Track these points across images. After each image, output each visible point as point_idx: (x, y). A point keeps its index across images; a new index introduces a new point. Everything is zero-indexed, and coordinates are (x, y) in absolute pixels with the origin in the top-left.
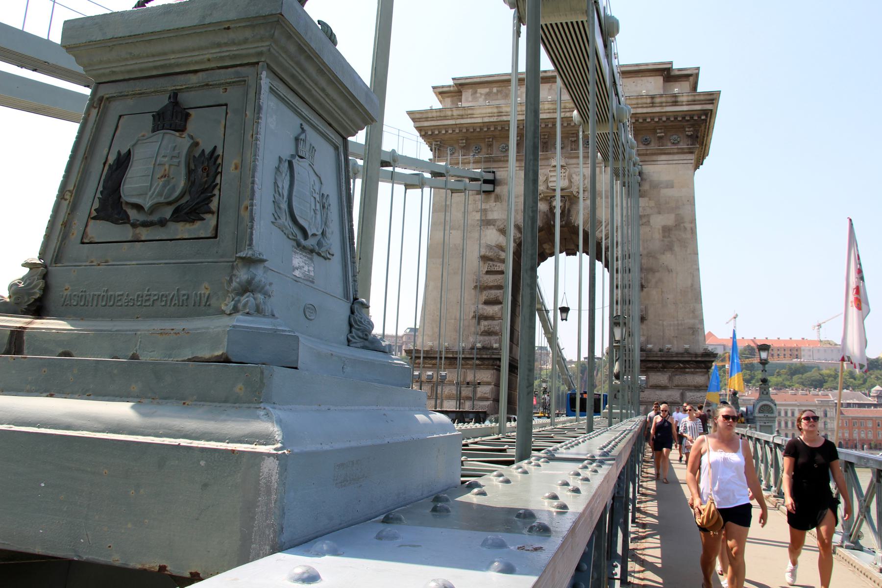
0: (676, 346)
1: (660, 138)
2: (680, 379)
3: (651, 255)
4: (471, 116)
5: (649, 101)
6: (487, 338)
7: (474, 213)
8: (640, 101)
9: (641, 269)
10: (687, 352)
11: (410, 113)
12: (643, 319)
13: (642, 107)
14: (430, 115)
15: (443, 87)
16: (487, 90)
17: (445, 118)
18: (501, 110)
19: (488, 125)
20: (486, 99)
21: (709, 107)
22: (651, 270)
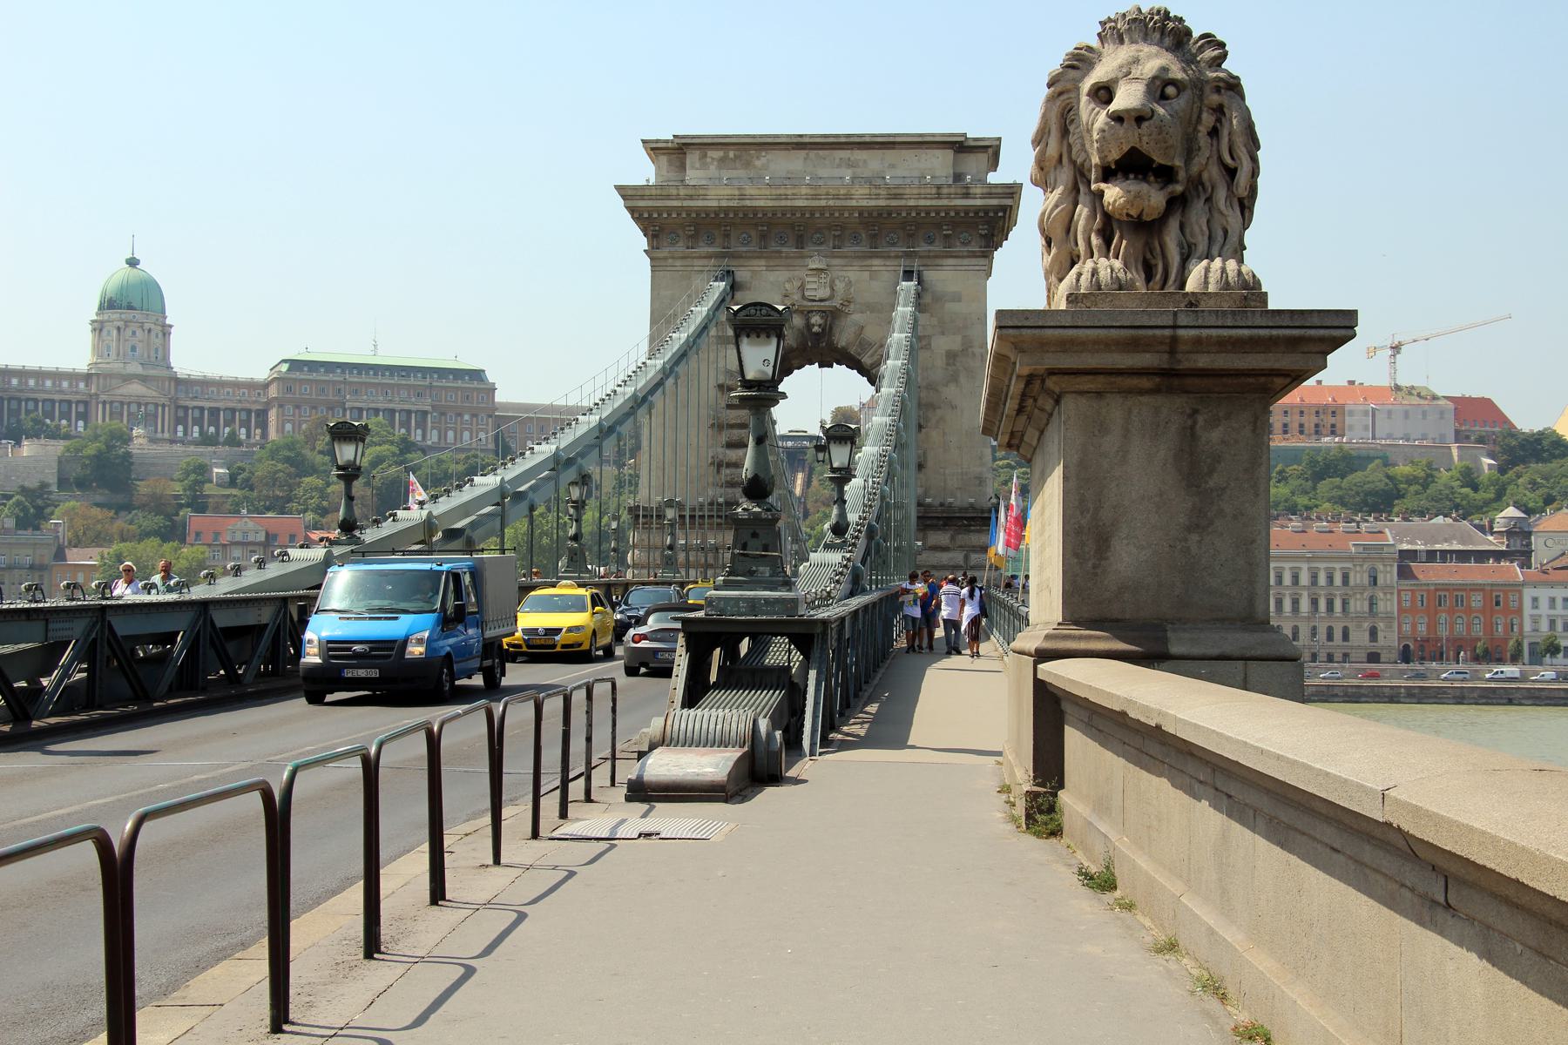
0: (960, 500)
2: (963, 539)
3: (931, 387)
4: (704, 197)
6: (730, 490)
9: (919, 405)
10: (972, 506)
11: (619, 188)
12: (920, 467)
15: (657, 141)
16: (721, 154)
17: (668, 197)
19: (727, 210)
20: (719, 168)
21: (1008, 202)
22: (932, 406)
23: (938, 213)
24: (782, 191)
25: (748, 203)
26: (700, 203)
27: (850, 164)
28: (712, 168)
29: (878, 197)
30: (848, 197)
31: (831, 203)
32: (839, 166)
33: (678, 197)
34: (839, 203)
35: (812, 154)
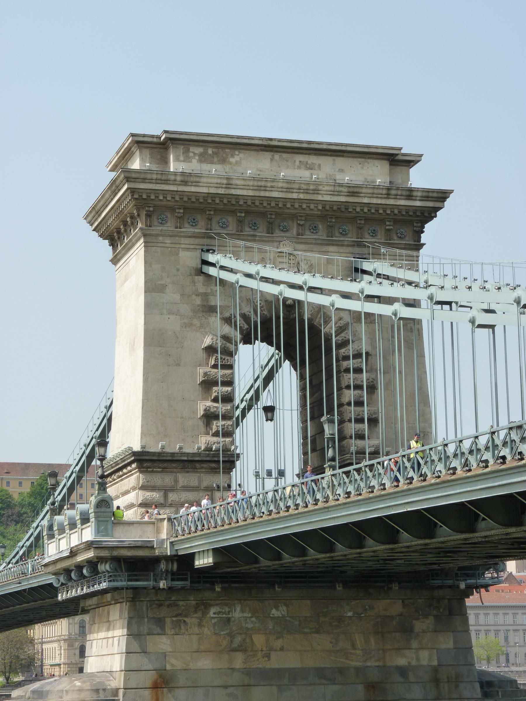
1: (389, 230)
4: (197, 184)
5: (385, 192)
7: (194, 297)
8: (376, 191)
13: (377, 197)
14: (149, 176)
15: (144, 136)
16: (200, 150)
18: (231, 182)
20: (200, 161)
21: (438, 205)
23: (385, 211)
24: (263, 184)
25: (233, 192)
26: (193, 189)
27: (310, 167)
28: (194, 161)
29: (339, 193)
30: (316, 191)
31: (302, 196)
32: (299, 168)
33: (174, 182)
34: (308, 197)
35: (277, 156)
